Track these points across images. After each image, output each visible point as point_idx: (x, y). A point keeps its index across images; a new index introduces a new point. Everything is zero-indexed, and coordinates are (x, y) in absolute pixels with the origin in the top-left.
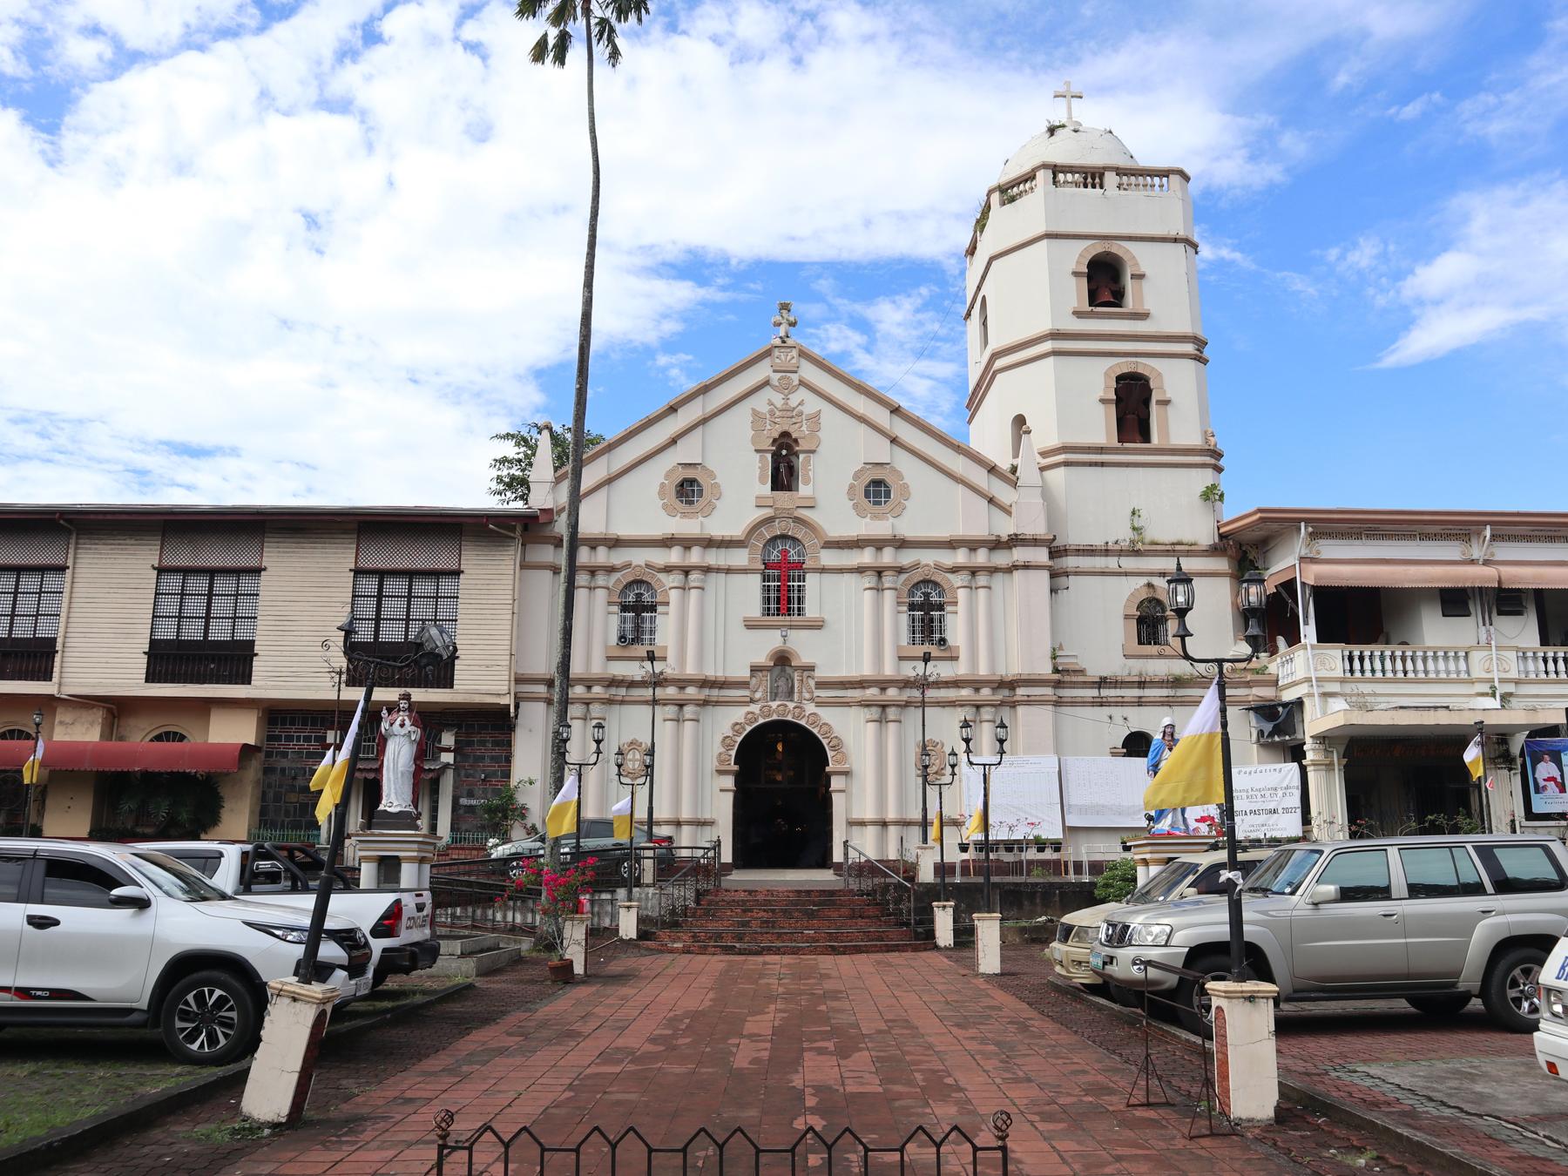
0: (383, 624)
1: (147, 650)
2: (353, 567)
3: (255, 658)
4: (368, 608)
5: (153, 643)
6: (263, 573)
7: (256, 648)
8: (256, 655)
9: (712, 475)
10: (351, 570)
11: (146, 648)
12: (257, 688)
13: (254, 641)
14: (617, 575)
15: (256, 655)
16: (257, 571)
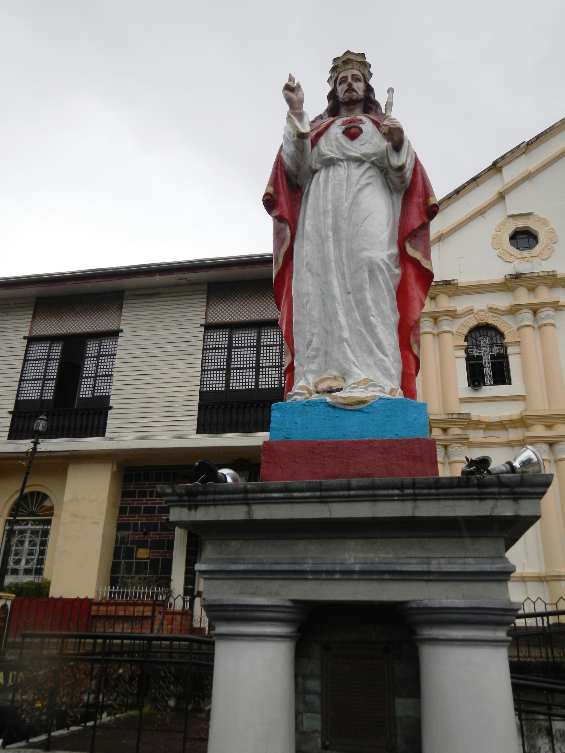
0: (233, 373)
1: (12, 410)
2: (203, 322)
3: (110, 412)
4: (220, 359)
5: (18, 403)
6: (120, 335)
7: (111, 402)
8: (111, 408)
9: (545, 222)
10: (201, 325)
11: (12, 407)
12: (112, 439)
13: (109, 396)
14: (461, 321)
15: (111, 408)
16: (114, 334)
